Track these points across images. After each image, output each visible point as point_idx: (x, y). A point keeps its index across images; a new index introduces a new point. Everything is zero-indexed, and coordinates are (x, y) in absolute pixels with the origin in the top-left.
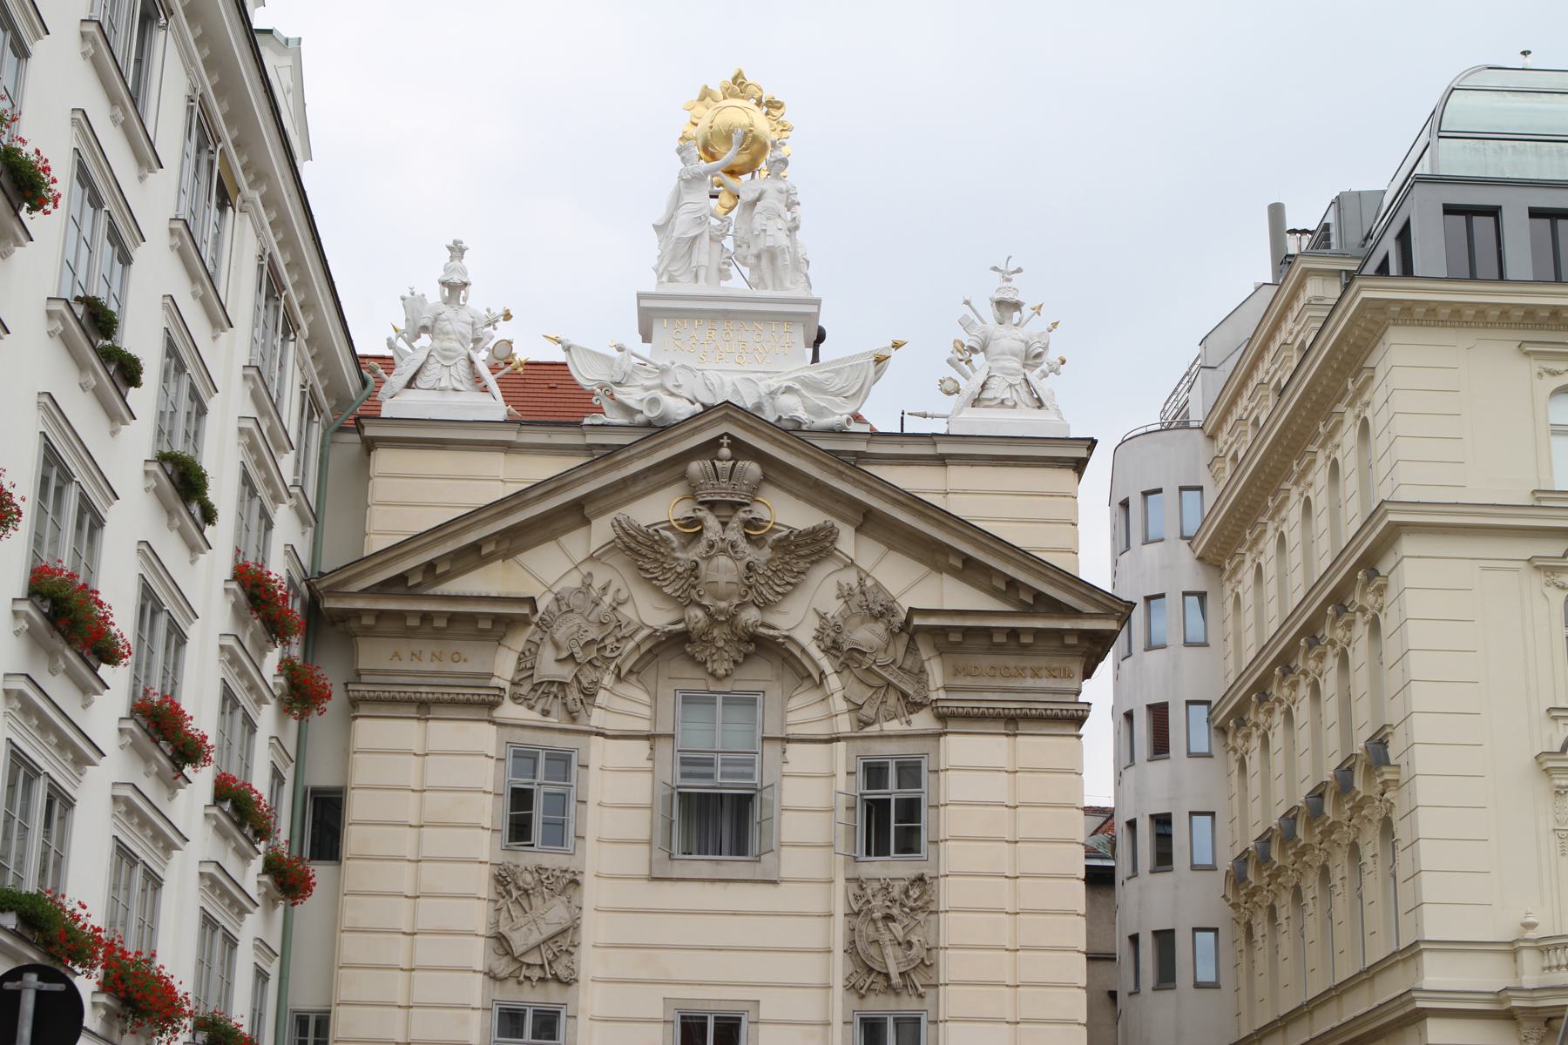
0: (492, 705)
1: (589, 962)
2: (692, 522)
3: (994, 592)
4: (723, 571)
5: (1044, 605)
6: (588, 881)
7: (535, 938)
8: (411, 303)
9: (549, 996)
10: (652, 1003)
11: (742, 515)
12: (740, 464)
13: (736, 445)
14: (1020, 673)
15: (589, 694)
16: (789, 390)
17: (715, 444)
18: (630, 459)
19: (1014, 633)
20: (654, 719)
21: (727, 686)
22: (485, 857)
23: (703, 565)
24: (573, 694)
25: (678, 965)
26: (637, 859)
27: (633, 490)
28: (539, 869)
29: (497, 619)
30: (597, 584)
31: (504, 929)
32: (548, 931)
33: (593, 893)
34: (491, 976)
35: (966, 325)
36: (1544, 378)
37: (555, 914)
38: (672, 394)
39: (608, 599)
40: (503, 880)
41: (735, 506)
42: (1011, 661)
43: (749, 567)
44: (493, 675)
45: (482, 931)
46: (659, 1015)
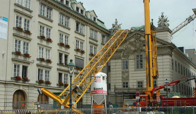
0: (121, 58)
1: (130, 78)
2: (135, 41)
3: (160, 44)
4: (138, 45)
5: (164, 44)
6: (130, 72)
7: (125, 76)
8: (113, 25)
9: (127, 81)
10: (135, 81)
11: (139, 40)
12: (138, 35)
13: (138, 33)
14: (163, 51)
15: (129, 56)
16: (142, 28)
17: (136, 34)
18: (129, 36)
19: (162, 47)
20: (134, 58)
21: (140, 54)
22: (121, 70)
23: (136, 44)
24: (127, 56)
25: (138, 78)
26: (133, 69)
27: (130, 38)
28: (125, 71)
29: (120, 51)
30: (128, 47)
31: (123, 76)
32: (127, 76)
33: (130, 72)
34: (122, 80)
35: (159, 19)
36: (10, 79)
37: (127, 74)
38: (132, 30)
39: (129, 48)
40: (123, 72)
41: (138, 39)
42: (162, 49)
43: (140, 44)
44: (120, 56)
45: (121, 76)
46: (136, 82)
